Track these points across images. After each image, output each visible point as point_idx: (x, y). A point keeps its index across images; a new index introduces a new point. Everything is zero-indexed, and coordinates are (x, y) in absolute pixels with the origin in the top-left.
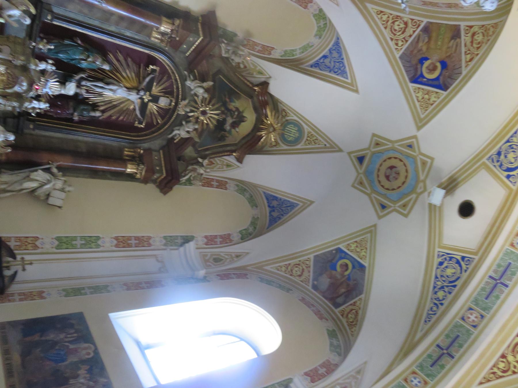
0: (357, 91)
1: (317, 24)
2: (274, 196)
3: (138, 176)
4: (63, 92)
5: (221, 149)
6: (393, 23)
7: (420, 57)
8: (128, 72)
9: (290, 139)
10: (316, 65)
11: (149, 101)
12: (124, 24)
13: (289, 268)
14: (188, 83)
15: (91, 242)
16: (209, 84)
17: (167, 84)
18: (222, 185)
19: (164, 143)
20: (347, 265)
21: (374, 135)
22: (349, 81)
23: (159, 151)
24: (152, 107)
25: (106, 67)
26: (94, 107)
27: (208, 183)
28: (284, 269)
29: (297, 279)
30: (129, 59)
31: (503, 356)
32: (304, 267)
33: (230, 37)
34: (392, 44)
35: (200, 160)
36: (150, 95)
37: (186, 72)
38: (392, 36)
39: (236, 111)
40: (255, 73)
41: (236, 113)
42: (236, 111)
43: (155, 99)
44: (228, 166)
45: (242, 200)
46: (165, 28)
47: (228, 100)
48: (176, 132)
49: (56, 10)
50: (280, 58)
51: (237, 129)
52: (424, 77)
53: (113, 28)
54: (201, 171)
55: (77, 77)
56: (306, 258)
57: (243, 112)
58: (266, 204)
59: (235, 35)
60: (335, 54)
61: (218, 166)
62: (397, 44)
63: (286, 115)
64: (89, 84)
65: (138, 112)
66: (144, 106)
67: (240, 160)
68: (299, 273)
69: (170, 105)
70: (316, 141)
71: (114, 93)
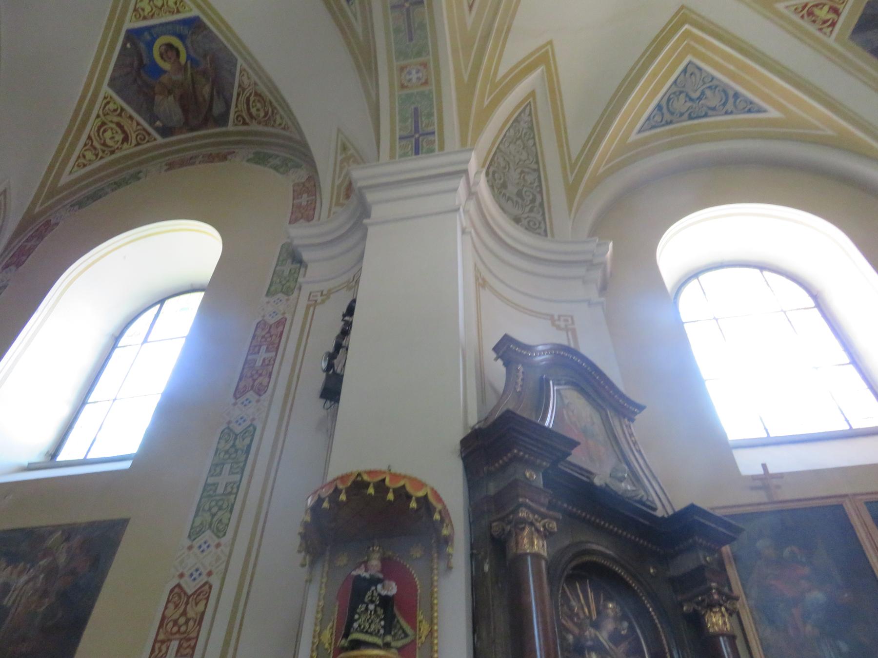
20: (170, 46)
28: (89, 155)
29: (128, 149)
32: (116, 119)
68: (119, 137)
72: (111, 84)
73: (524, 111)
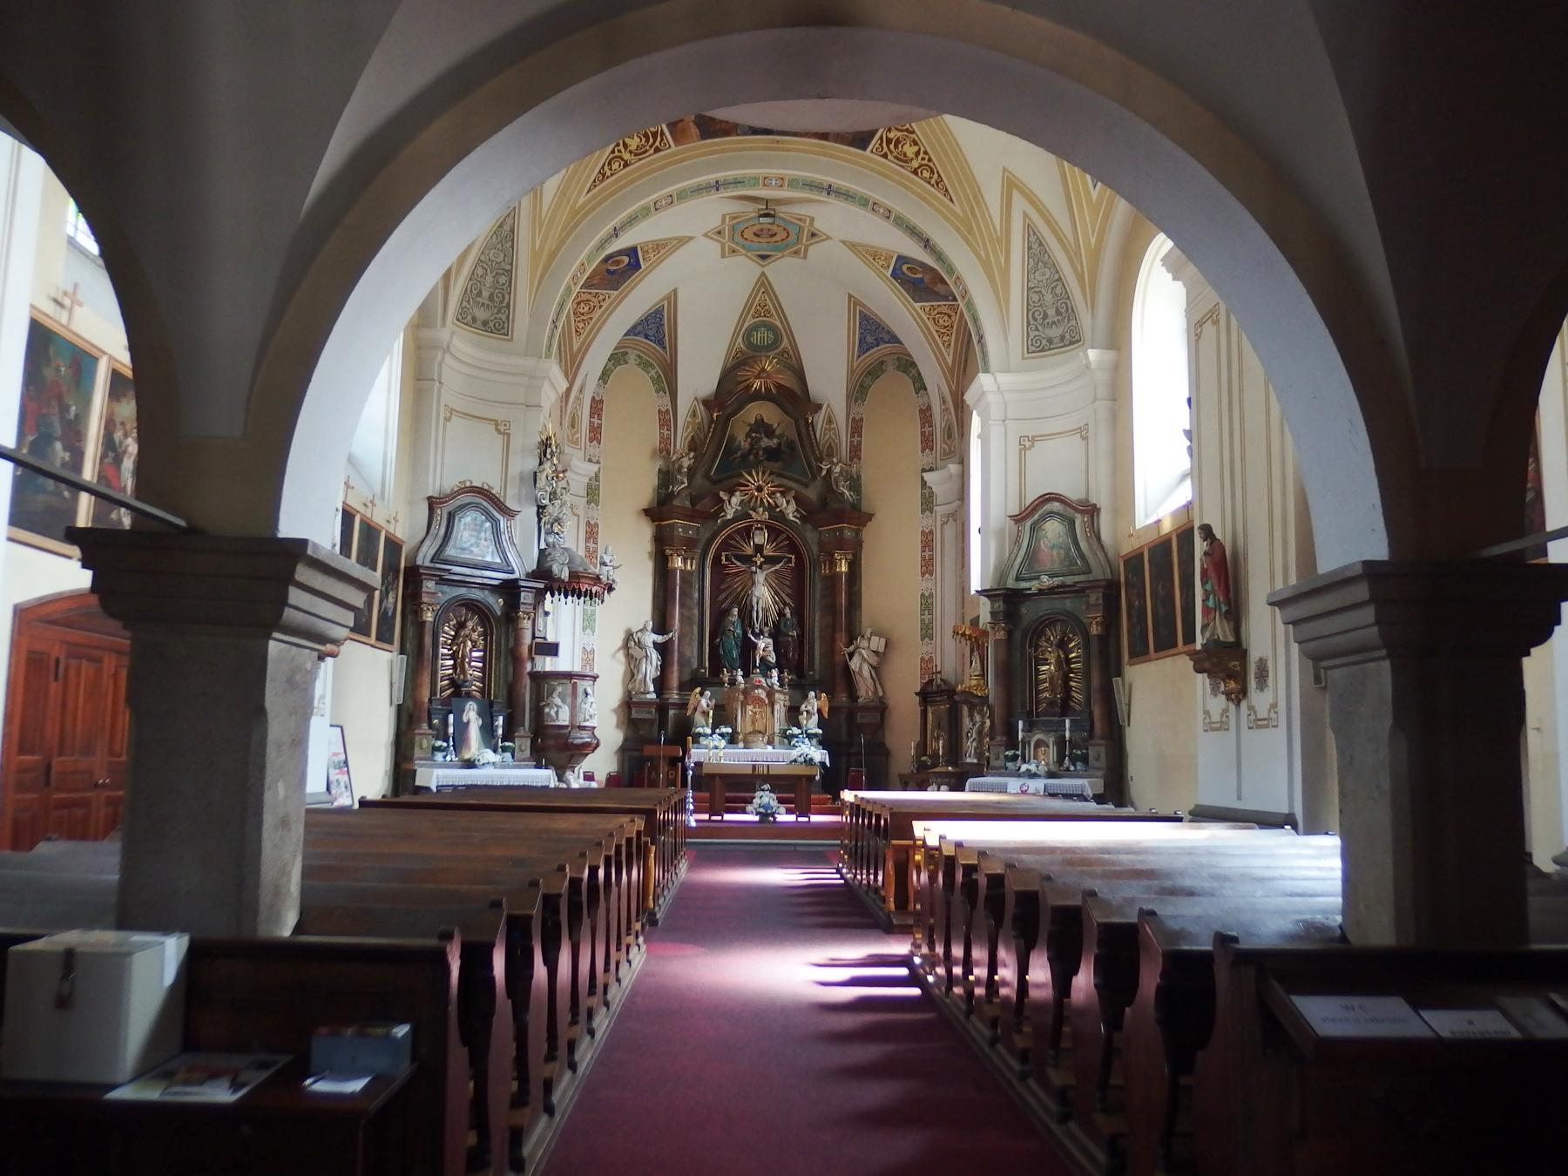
0: (675, 291)
5: (806, 443)
10: (661, 342)
15: (927, 603)
16: (722, 494)
18: (856, 427)
19: (809, 527)
21: (723, 256)
24: (768, 551)
26: (781, 614)
27: (855, 452)
31: (915, 172)
33: (666, 477)
34: (605, 305)
43: (759, 549)
44: (830, 421)
46: (678, 563)
53: (696, 612)
54: (838, 469)
66: (770, 560)
71: (763, 594)
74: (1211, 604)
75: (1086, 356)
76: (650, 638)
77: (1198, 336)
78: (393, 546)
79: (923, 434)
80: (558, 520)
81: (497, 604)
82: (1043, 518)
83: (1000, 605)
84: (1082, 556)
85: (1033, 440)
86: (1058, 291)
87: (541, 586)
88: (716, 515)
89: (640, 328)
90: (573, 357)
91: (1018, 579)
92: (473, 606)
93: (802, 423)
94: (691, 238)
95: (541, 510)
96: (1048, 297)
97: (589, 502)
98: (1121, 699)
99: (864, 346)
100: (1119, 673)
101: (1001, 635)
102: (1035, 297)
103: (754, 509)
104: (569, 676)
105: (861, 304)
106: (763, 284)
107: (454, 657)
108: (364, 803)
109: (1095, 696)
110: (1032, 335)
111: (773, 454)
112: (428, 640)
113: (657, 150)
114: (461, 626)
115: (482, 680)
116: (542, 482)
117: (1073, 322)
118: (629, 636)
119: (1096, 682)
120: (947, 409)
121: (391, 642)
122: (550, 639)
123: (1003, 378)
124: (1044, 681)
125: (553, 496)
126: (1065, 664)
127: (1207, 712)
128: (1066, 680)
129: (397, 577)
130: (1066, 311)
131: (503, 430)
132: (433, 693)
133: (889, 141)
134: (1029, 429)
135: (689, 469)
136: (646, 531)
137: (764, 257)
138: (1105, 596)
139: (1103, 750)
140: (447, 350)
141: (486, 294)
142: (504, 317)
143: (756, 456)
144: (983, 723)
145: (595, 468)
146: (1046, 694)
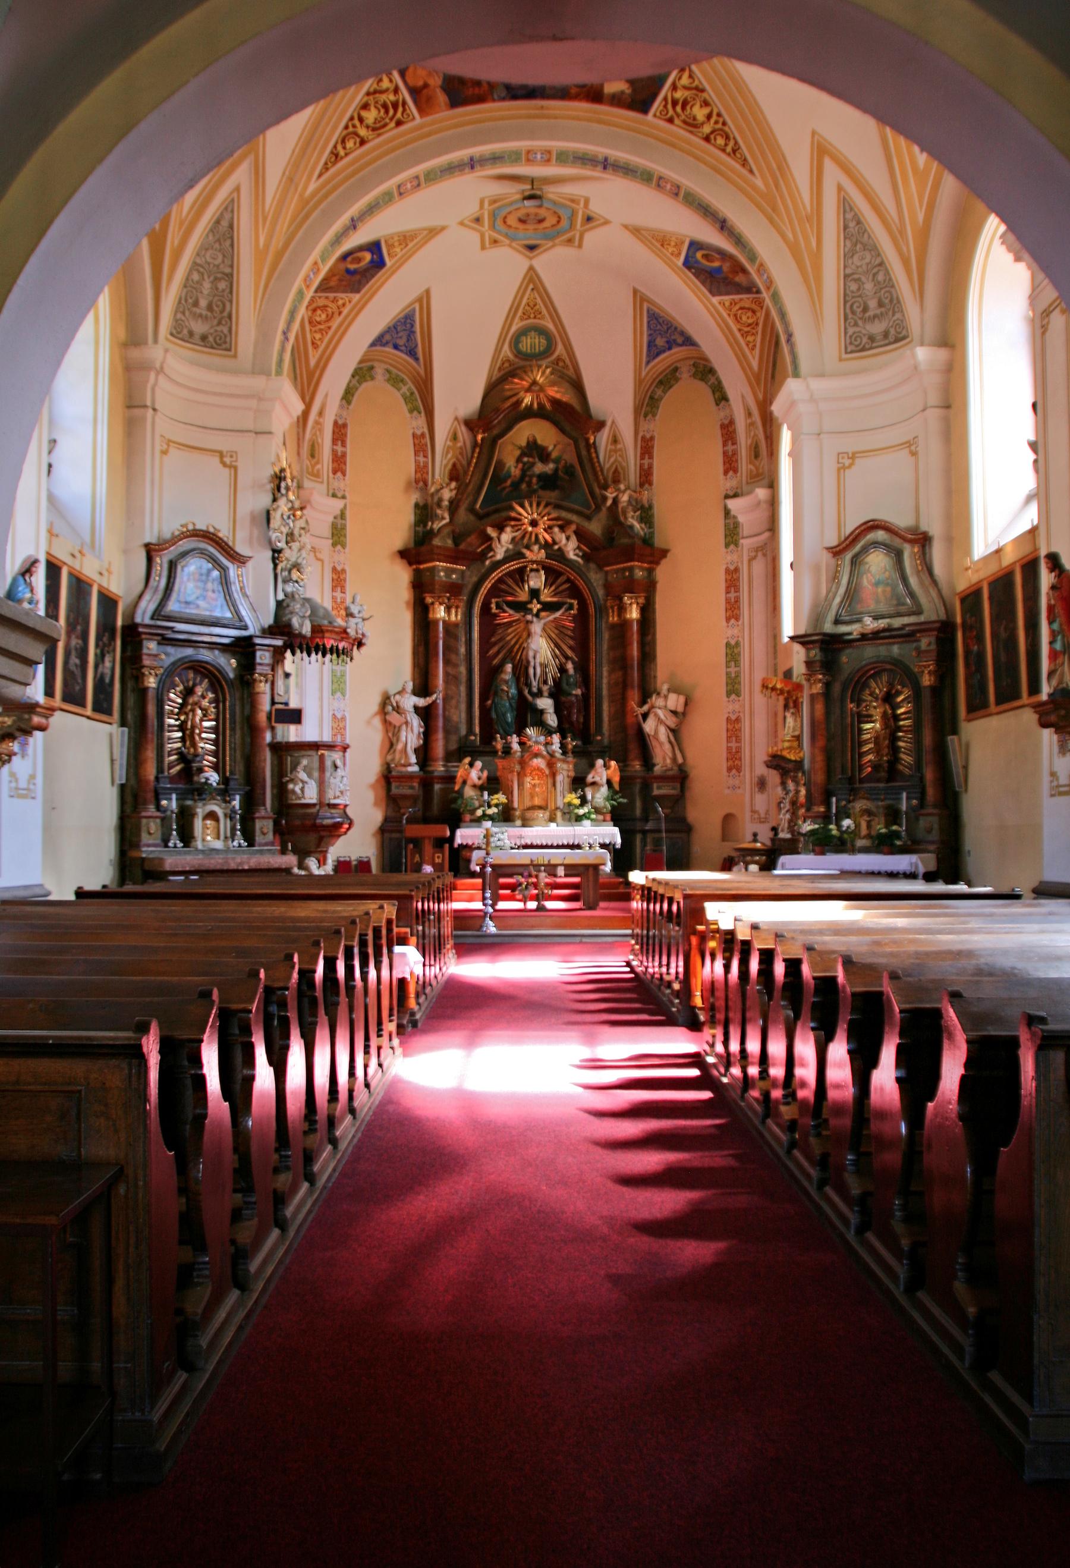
0: (428, 292)
1: (357, 389)
2: (649, 346)
3: (641, 601)
4: (551, 710)
5: (588, 467)
6: (319, 323)
7: (348, 277)
8: (508, 638)
9: (544, 342)
10: (412, 353)
11: (539, 602)
12: (453, 657)
13: (746, 329)
14: (500, 555)
15: (733, 653)
16: (490, 531)
17: (510, 582)
18: (646, 448)
19: (592, 566)
21: (483, 248)
22: (417, 306)
23: (607, 573)
24: (546, 596)
25: (509, 667)
26: (562, 670)
27: (646, 477)
28: (750, 338)
30: (493, 640)
31: (707, 139)
32: (737, 307)
33: (424, 513)
34: (345, 311)
35: (609, 502)
36: (531, 602)
37: (487, 563)
38: (336, 314)
39: (522, 462)
40: (459, 445)
41: (525, 459)
42: (522, 462)
43: (535, 593)
44: (615, 441)
45: (669, 400)
46: (440, 612)
47: (509, 483)
48: (572, 556)
49: (463, 731)
50: (423, 414)
51: (550, 448)
52: (372, 258)
53: (463, 669)
54: (625, 498)
55: (530, 698)
56: (720, 308)
57: (520, 448)
58: (667, 354)
59: (417, 505)
60: (388, 337)
61: (620, 459)
62: (344, 305)
63: (508, 361)
64: (535, 684)
65: (558, 614)
66: (549, 607)
67: (601, 425)
68: (750, 314)
69: (537, 570)
70: (531, 304)
71: (541, 648)
72: (713, 295)
73: (845, 212)
74: (1058, 646)
75: (914, 356)
76: (410, 701)
77: (1044, 329)
78: (108, 602)
79: (725, 453)
80: (297, 566)
81: (229, 665)
82: (865, 550)
83: (815, 653)
84: (912, 595)
85: (853, 457)
86: (880, 277)
87: (279, 643)
88: (483, 556)
89: (388, 337)
90: (311, 375)
91: (837, 622)
92: (201, 669)
93: (582, 445)
94: (443, 229)
95: (276, 552)
96: (869, 286)
97: (334, 545)
98: (956, 759)
99: (653, 351)
100: (955, 731)
101: (818, 688)
102: (853, 287)
103: (528, 547)
104: (315, 746)
105: (650, 301)
106: (532, 279)
107: (182, 727)
108: (81, 894)
109: (928, 757)
110: (851, 331)
111: (548, 482)
112: (151, 709)
113: (399, 123)
114: (188, 692)
115: (215, 754)
116: (276, 522)
117: (898, 316)
118: (386, 700)
119: (928, 739)
120: (752, 424)
121: (109, 712)
122: (293, 705)
123: (818, 385)
124: (867, 742)
125: (290, 537)
126: (891, 721)
127: (1053, 774)
128: (894, 739)
129: (113, 638)
130: (890, 304)
131: (228, 462)
132: (160, 770)
133: (675, 103)
134: (850, 444)
135: (451, 502)
136: (402, 575)
137: (531, 248)
138: (939, 640)
139: (934, 820)
140: (161, 371)
141: (203, 303)
142: (226, 331)
143: (529, 484)
144: (797, 792)
145: (338, 504)
146: (871, 757)
